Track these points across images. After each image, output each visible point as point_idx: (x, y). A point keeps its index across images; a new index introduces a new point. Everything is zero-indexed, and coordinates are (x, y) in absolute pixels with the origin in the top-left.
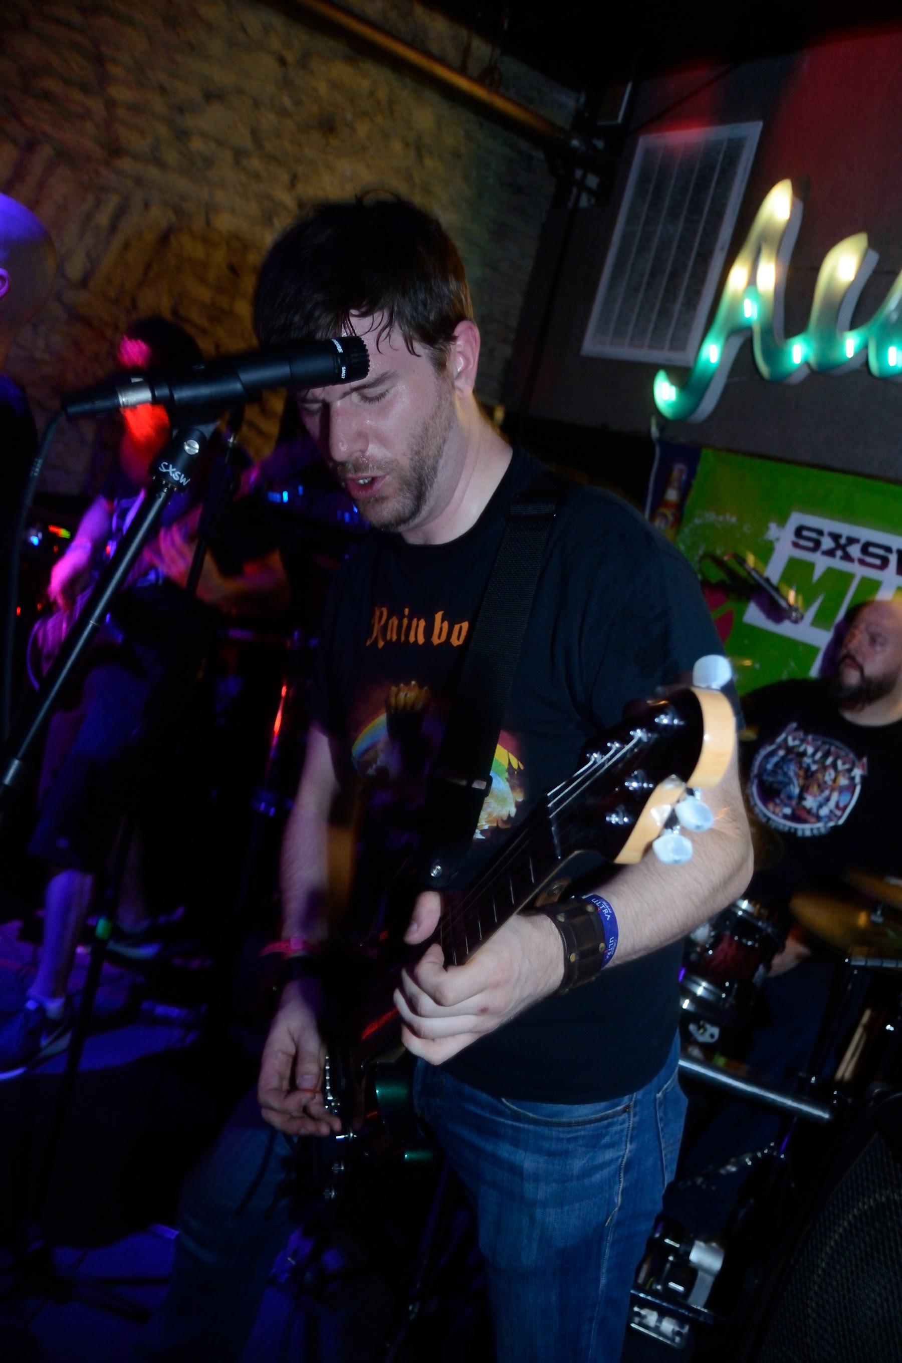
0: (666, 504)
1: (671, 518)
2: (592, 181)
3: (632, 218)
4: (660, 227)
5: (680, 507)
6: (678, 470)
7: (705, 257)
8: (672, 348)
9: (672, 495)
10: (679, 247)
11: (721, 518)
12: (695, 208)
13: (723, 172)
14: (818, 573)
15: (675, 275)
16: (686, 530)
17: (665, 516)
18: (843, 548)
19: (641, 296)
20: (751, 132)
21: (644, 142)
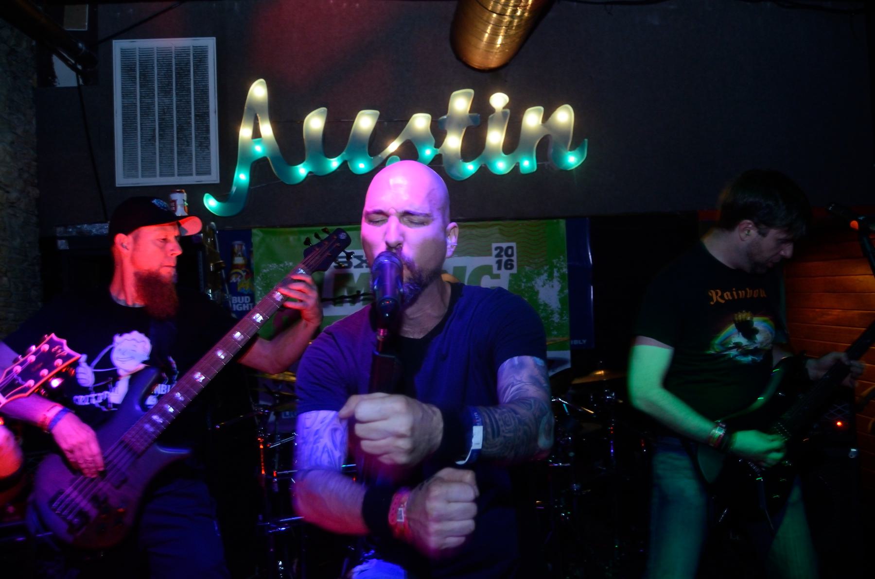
0: (237, 266)
1: (244, 274)
2: (80, 67)
3: (127, 94)
4: (156, 99)
5: (248, 266)
6: (238, 245)
7: (203, 117)
8: (198, 174)
9: (239, 260)
10: (178, 112)
11: (282, 265)
12: (183, 88)
13: (196, 67)
14: (356, 278)
15: (183, 129)
16: (258, 279)
17: (238, 273)
18: (363, 261)
19: (157, 143)
20: (210, 43)
21: (119, 46)
